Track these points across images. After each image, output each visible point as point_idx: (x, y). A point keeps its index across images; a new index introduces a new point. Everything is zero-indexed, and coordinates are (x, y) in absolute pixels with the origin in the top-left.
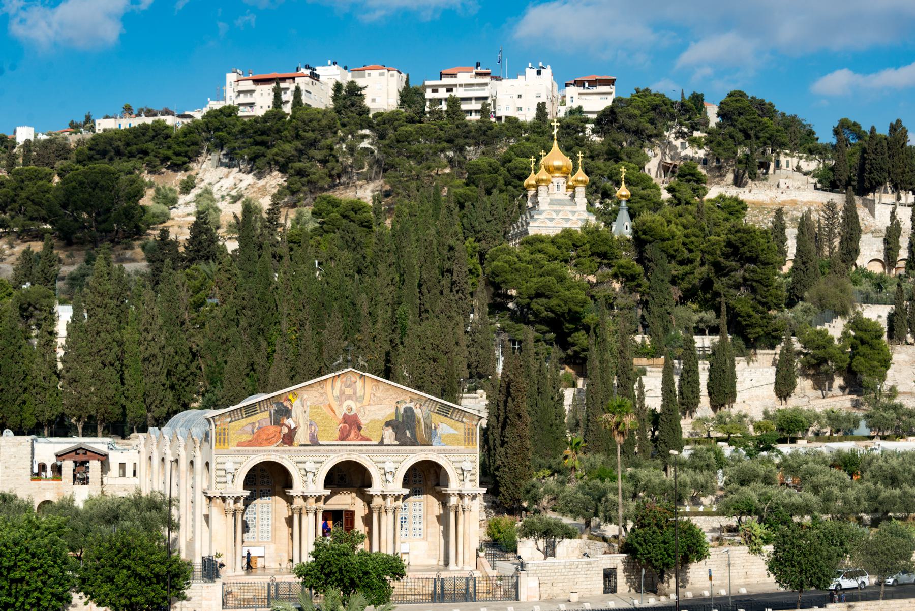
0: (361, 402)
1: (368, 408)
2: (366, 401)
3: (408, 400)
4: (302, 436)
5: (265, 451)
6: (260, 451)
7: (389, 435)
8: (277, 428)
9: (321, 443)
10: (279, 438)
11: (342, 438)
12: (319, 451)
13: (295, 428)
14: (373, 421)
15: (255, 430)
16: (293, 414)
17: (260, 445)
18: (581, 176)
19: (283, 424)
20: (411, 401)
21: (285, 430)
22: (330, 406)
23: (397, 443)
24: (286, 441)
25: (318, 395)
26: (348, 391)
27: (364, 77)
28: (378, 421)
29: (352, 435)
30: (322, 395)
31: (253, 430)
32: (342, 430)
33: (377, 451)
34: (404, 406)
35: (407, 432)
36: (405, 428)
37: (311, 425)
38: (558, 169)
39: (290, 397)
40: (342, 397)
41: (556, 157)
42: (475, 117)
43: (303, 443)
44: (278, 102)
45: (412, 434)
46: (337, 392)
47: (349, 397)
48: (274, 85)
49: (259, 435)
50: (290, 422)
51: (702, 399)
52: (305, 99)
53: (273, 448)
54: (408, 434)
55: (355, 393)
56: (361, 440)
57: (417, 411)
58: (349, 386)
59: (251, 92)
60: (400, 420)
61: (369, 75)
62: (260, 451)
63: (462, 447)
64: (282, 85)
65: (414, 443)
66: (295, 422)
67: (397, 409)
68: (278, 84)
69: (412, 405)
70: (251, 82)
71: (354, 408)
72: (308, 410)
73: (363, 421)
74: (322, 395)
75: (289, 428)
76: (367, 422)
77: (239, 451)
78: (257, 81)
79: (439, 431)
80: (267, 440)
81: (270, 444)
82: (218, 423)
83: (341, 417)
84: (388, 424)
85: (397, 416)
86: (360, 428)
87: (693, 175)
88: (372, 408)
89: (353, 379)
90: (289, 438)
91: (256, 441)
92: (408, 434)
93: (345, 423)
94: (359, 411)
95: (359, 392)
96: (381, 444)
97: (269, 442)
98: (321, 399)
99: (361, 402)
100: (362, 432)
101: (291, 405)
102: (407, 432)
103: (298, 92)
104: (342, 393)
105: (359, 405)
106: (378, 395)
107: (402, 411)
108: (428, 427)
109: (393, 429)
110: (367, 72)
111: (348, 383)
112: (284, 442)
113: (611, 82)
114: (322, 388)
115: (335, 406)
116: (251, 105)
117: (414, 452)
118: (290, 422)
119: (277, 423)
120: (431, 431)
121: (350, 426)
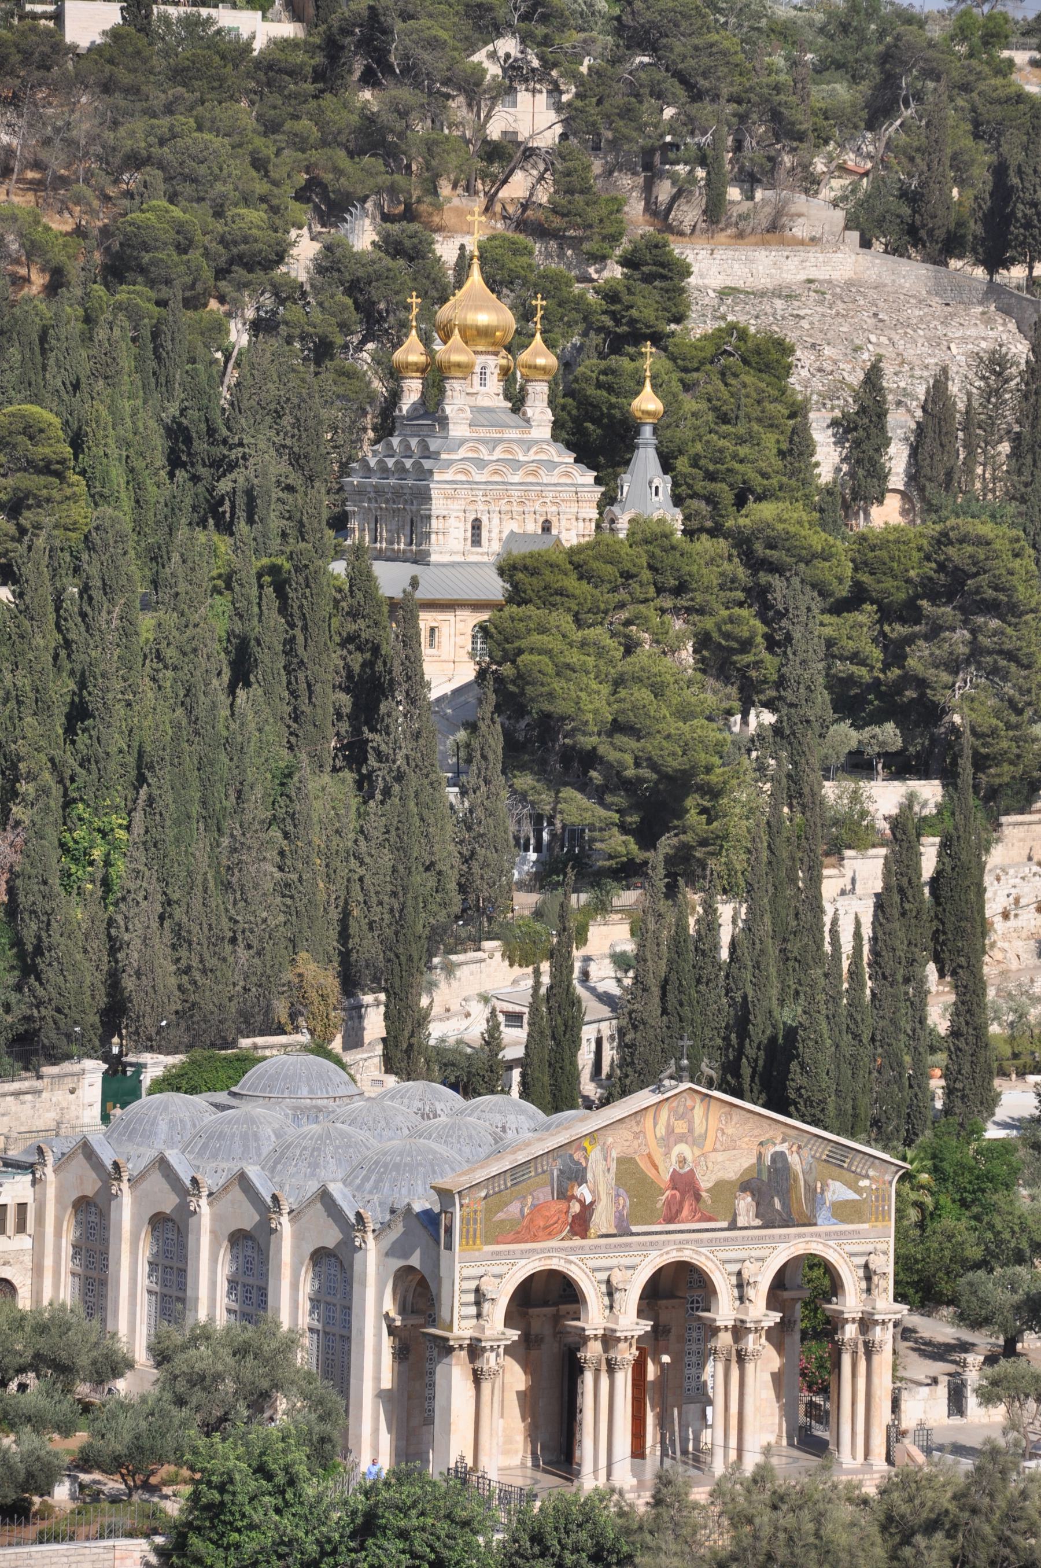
0: (701, 1146)
1: (713, 1156)
2: (709, 1145)
3: (778, 1141)
4: (602, 1220)
5: (542, 1251)
6: (534, 1251)
7: (745, 1204)
8: (562, 1205)
9: (634, 1229)
10: (564, 1223)
11: (670, 1220)
12: (629, 1245)
13: (592, 1203)
14: (720, 1186)
15: (526, 1211)
16: (589, 1176)
17: (534, 1239)
18: (539, 355)
19: (573, 1197)
20: (784, 1141)
21: (576, 1208)
22: (649, 1156)
23: (758, 1222)
24: (577, 1228)
25: (630, 1137)
26: (681, 1127)
28: (729, 1182)
29: (685, 1213)
30: (636, 1136)
31: (522, 1211)
32: (668, 1203)
33: (726, 1239)
34: (772, 1150)
35: (776, 1200)
36: (775, 1195)
37: (618, 1195)
38: (485, 333)
39: (586, 1144)
40: (671, 1137)
43: (604, 1231)
45: (783, 1205)
46: (661, 1130)
47: (681, 1139)
49: (532, 1221)
50: (584, 1192)
53: (554, 1243)
54: (778, 1205)
55: (691, 1130)
56: (700, 1220)
57: (793, 1159)
58: (681, 1117)
60: (765, 1177)
62: (534, 1251)
63: (866, 1226)
65: (787, 1222)
66: (592, 1192)
67: (760, 1156)
69: (783, 1148)
71: (689, 1158)
72: (613, 1166)
73: (705, 1183)
74: (636, 1136)
75: (582, 1203)
76: (710, 1185)
77: (498, 1253)
79: (830, 1197)
80: (545, 1228)
81: (550, 1236)
82: (466, 1201)
83: (668, 1178)
84: (746, 1186)
85: (760, 1171)
86: (698, 1197)
88: (720, 1157)
89: (689, 1103)
90: (580, 1225)
91: (526, 1231)
92: (778, 1205)
93: (674, 1188)
94: (697, 1164)
95: (699, 1130)
96: (733, 1226)
97: (549, 1233)
98: (636, 1143)
99: (701, 1146)
100: (701, 1205)
101: (586, 1159)
102: (776, 1200)
104: (670, 1130)
105: (697, 1152)
106: (730, 1131)
107: (768, 1161)
108: (811, 1190)
109: (753, 1195)
111: (681, 1110)
112: (573, 1233)
114: (638, 1123)
115: (658, 1159)
117: (785, 1239)
118: (584, 1192)
119: (564, 1195)
120: (814, 1197)
121: (683, 1195)
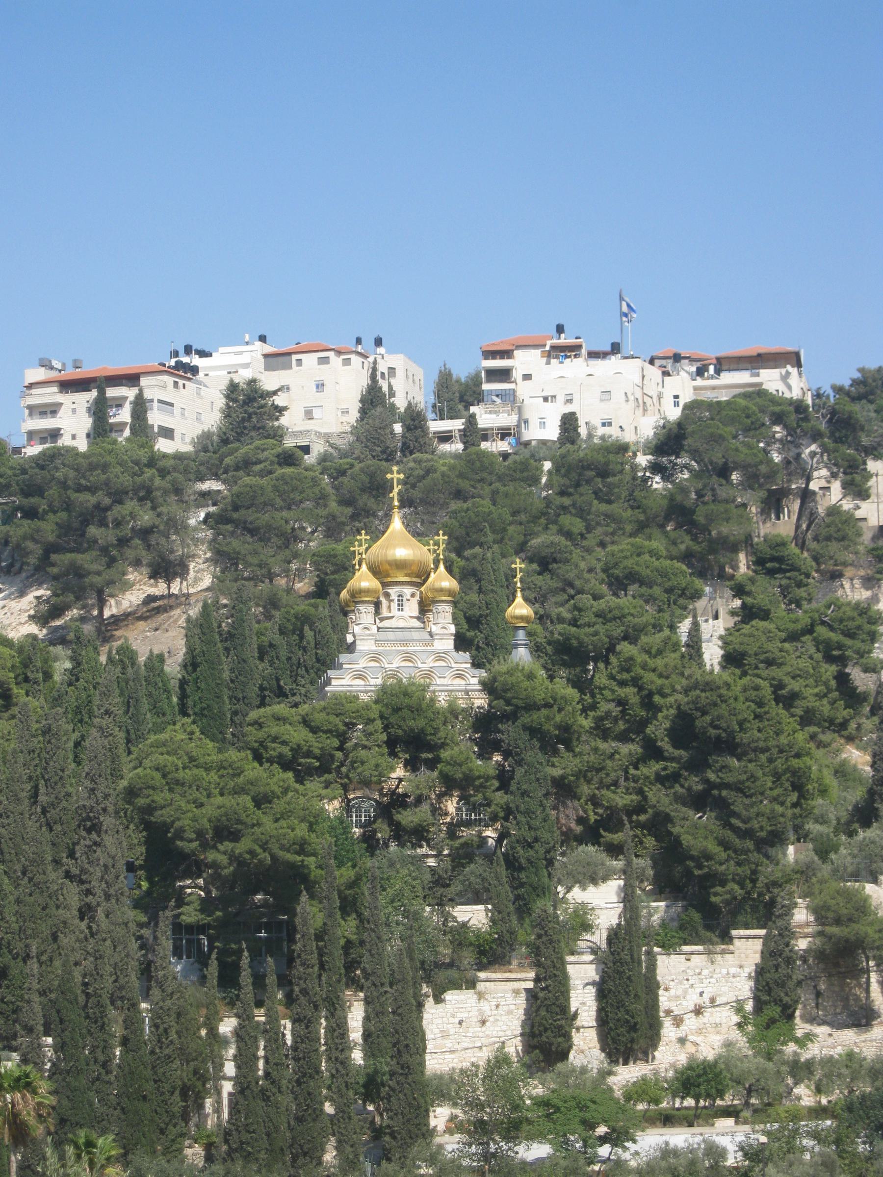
18: (443, 580)
27: (290, 367)
38: (401, 565)
41: (398, 542)
42: (457, 447)
44: (101, 427)
48: (94, 393)
51: (577, 1038)
52: (156, 418)
59: (52, 410)
61: (299, 362)
64: (112, 392)
68: (102, 392)
70: (55, 389)
78: (69, 386)
87: (780, 560)
103: (140, 407)
110: (295, 357)
113: (795, 359)
116: (55, 434)
